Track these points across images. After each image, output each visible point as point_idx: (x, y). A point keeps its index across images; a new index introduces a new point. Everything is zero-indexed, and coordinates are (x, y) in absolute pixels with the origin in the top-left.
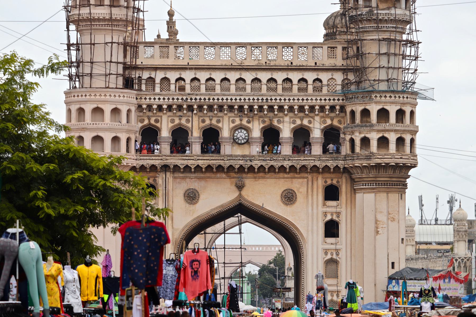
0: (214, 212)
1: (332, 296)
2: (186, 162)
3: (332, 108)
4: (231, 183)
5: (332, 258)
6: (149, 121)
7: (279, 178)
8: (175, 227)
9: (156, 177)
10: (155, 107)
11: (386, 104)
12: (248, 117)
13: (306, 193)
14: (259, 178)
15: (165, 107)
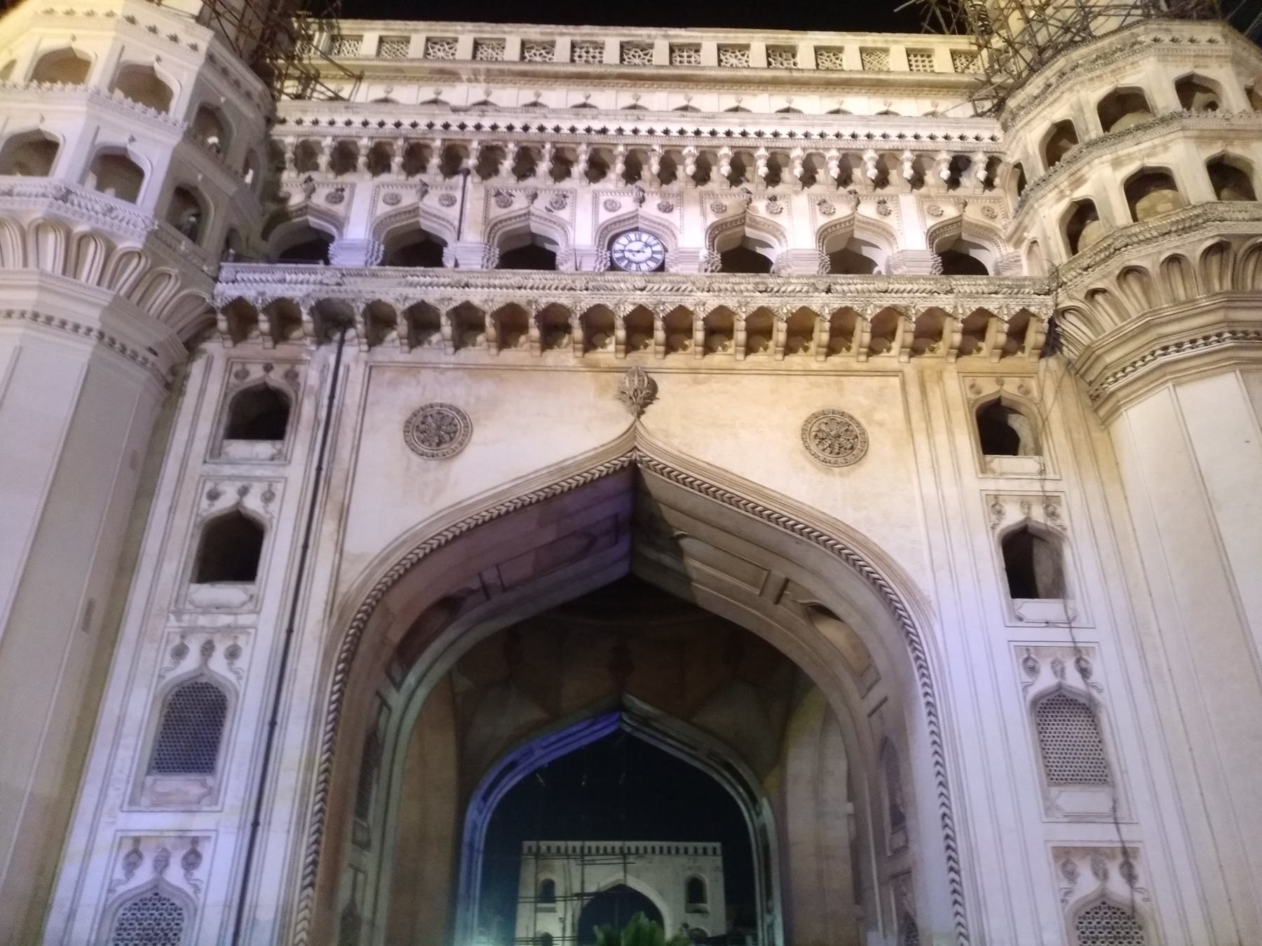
0: (527, 492)
1: (1102, 875)
2: (416, 295)
3: (959, 165)
4: (602, 390)
5: (1060, 687)
6: (309, 197)
7: (789, 373)
8: (348, 547)
9: (301, 361)
10: (327, 142)
11: (1201, 61)
12: (663, 195)
13: (901, 425)
14: (712, 371)
15: (365, 143)
